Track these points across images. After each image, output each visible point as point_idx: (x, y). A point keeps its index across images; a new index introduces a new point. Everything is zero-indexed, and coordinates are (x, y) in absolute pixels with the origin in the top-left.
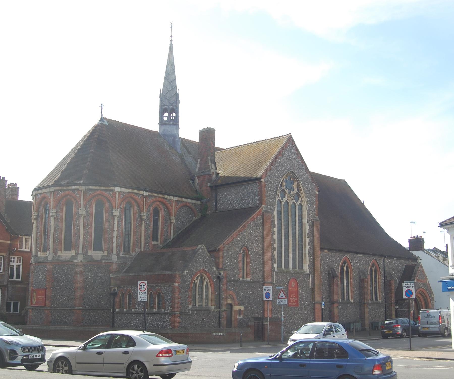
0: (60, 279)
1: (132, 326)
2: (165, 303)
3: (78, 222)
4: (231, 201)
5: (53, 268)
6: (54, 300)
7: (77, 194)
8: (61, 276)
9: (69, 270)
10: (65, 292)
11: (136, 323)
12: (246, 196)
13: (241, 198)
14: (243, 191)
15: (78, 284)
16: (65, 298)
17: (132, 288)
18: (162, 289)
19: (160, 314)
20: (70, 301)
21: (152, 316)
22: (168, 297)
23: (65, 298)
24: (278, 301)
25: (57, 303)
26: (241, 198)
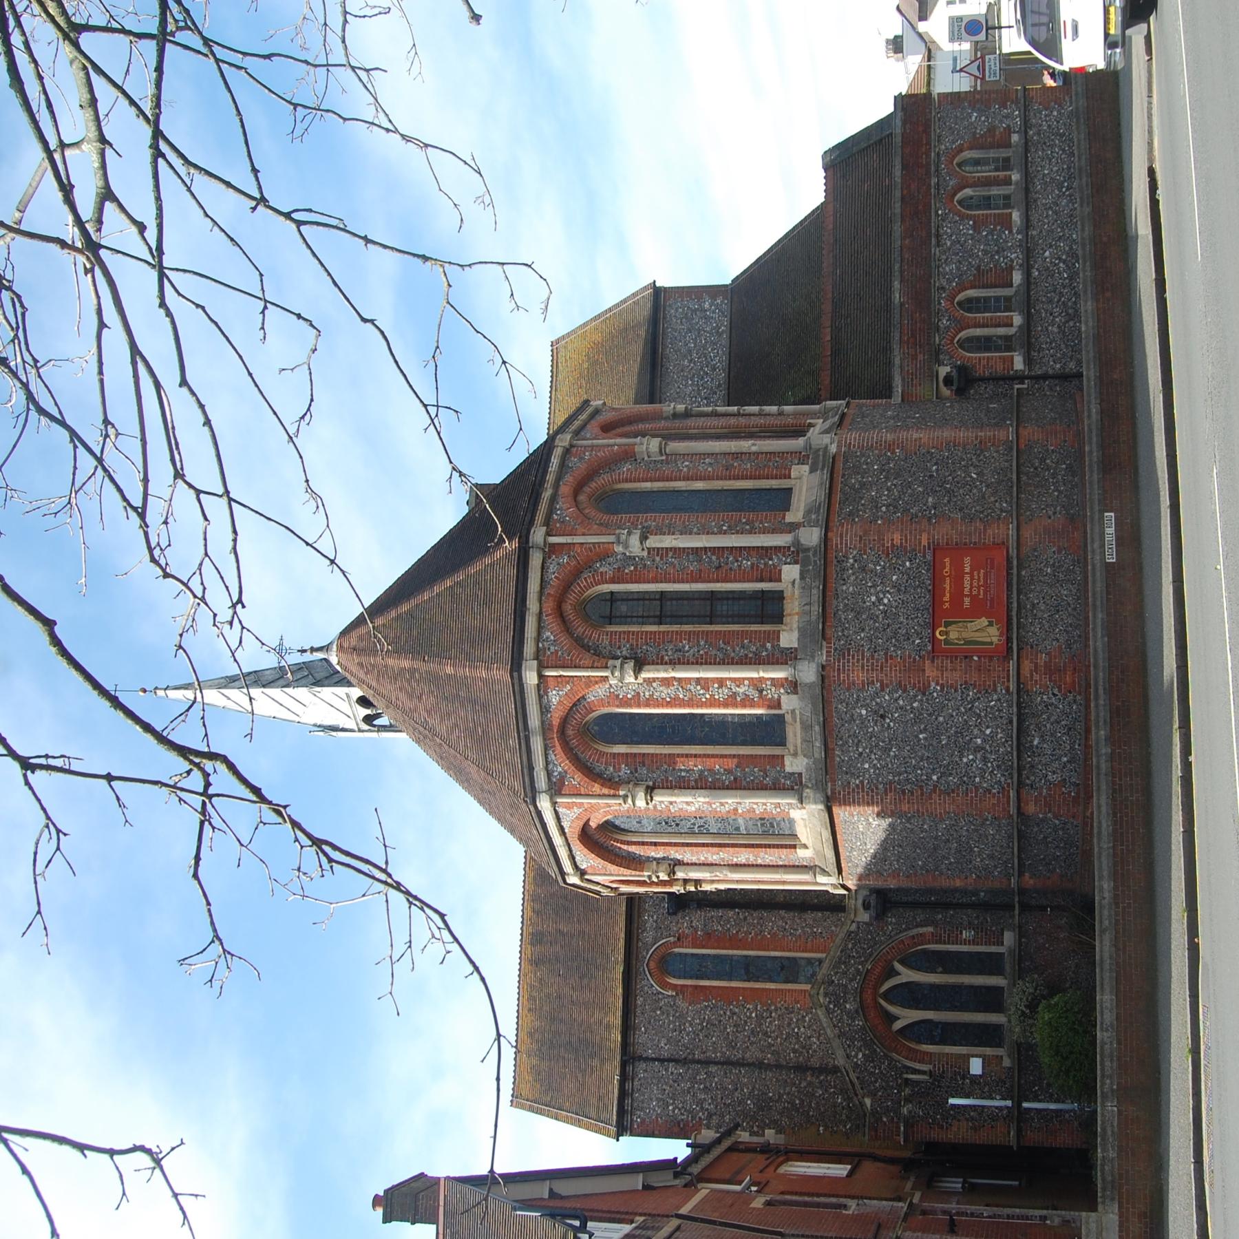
1: (1071, 278)
2: (991, 130)
3: (687, 463)
5: (853, 520)
6: (982, 512)
7: (581, 459)
8: (886, 493)
9: (865, 467)
11: (1060, 259)
13: (698, 358)
14: (680, 350)
15: (920, 439)
16: (974, 476)
17: (943, 288)
19: (1027, 150)
22: (973, 119)
23: (974, 476)
24: (990, 77)
26: (698, 358)
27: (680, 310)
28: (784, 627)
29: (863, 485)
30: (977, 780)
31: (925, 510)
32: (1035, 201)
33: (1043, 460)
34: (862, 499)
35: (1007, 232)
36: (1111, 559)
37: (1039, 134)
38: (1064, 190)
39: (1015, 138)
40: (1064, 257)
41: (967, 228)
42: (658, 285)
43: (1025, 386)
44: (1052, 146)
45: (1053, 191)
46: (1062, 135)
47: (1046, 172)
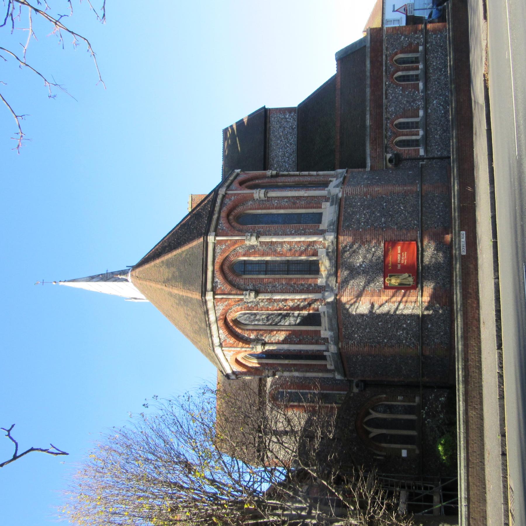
0: (368, 216)
2: (410, 44)
3: (276, 201)
4: (285, 156)
5: (349, 229)
6: (405, 225)
7: (230, 199)
9: (354, 204)
10: (391, 208)
11: (440, 104)
12: (283, 132)
13: (284, 139)
16: (402, 208)
18: (390, 54)
20: (407, 199)
21: (429, 69)
22: (402, 39)
23: (402, 208)
25: (410, 219)
26: (284, 139)
27: (276, 118)
28: (319, 276)
29: (353, 212)
30: (404, 341)
31: (381, 225)
32: (430, 78)
33: (432, 201)
34: (353, 219)
35: (417, 92)
36: (464, 253)
37: (431, 46)
38: (442, 72)
39: (421, 48)
40: (442, 103)
41: (399, 91)
42: (266, 107)
43: (424, 163)
44: (437, 52)
45: (437, 73)
46: (442, 46)
47: (434, 64)
